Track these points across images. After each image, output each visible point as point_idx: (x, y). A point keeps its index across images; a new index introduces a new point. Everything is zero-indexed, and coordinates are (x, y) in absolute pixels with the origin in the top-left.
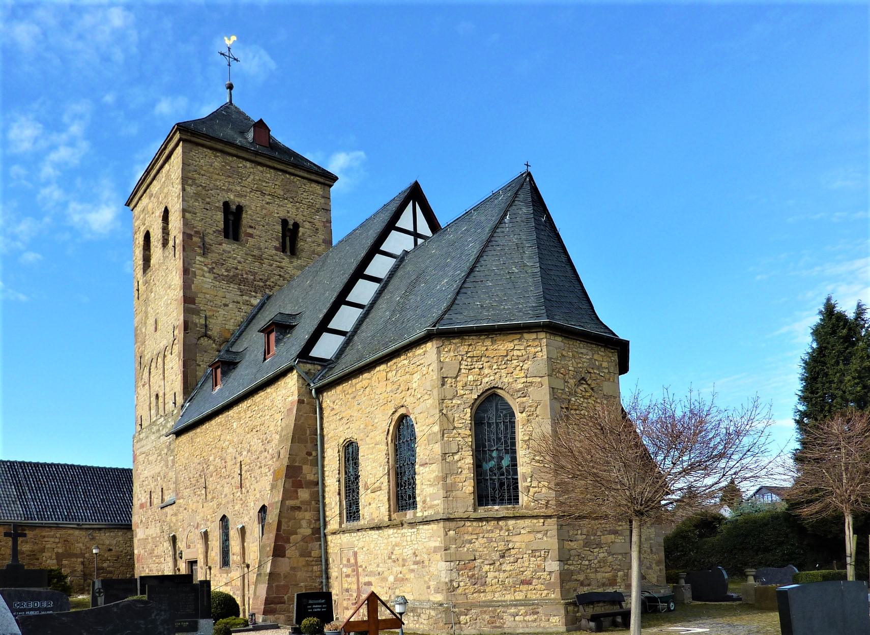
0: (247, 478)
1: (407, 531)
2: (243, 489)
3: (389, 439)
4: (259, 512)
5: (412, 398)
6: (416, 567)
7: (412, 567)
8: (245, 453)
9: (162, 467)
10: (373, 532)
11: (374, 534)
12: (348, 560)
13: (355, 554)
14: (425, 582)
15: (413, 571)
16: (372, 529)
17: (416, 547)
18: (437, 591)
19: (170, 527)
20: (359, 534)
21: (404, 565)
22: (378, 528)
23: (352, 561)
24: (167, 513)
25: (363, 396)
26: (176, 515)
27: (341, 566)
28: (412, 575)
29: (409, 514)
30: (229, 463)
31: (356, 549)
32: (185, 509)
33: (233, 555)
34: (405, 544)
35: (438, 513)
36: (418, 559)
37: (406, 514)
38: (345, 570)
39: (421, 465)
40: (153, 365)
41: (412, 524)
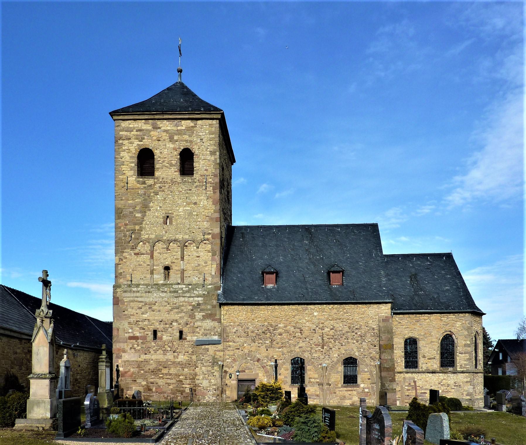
0: (331, 342)
1: (452, 375)
2: (325, 347)
3: (440, 341)
4: (344, 360)
5: (456, 330)
6: (456, 387)
7: (454, 387)
8: (326, 330)
9: (180, 317)
10: (429, 374)
11: (430, 375)
12: (410, 384)
13: (415, 382)
14: (461, 392)
15: (454, 389)
16: (427, 373)
17: (456, 380)
18: (467, 395)
19: (214, 358)
20: (419, 374)
21: (448, 387)
22: (433, 372)
23: (413, 384)
24: (208, 349)
25: (424, 322)
26: (224, 351)
27: (404, 386)
28: (453, 390)
29: (451, 369)
30: (306, 333)
31: (415, 380)
32: (239, 349)
33: (310, 378)
34: (449, 379)
35: (469, 370)
36: (456, 384)
37: (448, 369)
38: (406, 388)
39: (460, 353)
40: (159, 246)
41: (454, 373)
